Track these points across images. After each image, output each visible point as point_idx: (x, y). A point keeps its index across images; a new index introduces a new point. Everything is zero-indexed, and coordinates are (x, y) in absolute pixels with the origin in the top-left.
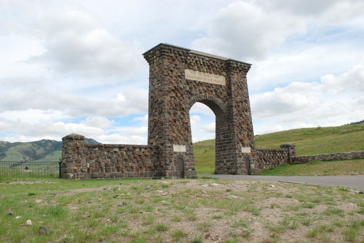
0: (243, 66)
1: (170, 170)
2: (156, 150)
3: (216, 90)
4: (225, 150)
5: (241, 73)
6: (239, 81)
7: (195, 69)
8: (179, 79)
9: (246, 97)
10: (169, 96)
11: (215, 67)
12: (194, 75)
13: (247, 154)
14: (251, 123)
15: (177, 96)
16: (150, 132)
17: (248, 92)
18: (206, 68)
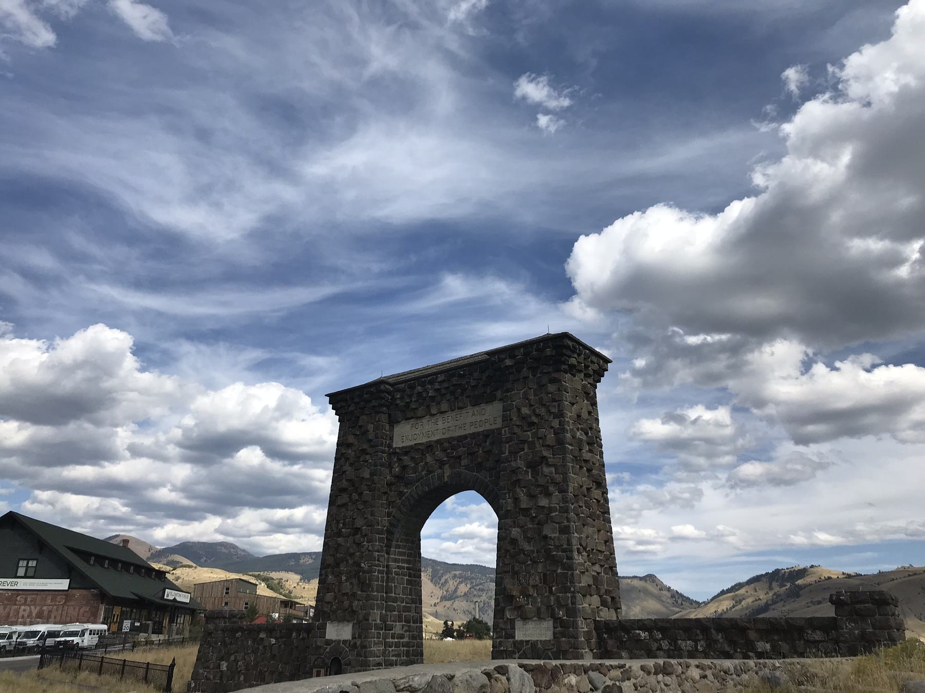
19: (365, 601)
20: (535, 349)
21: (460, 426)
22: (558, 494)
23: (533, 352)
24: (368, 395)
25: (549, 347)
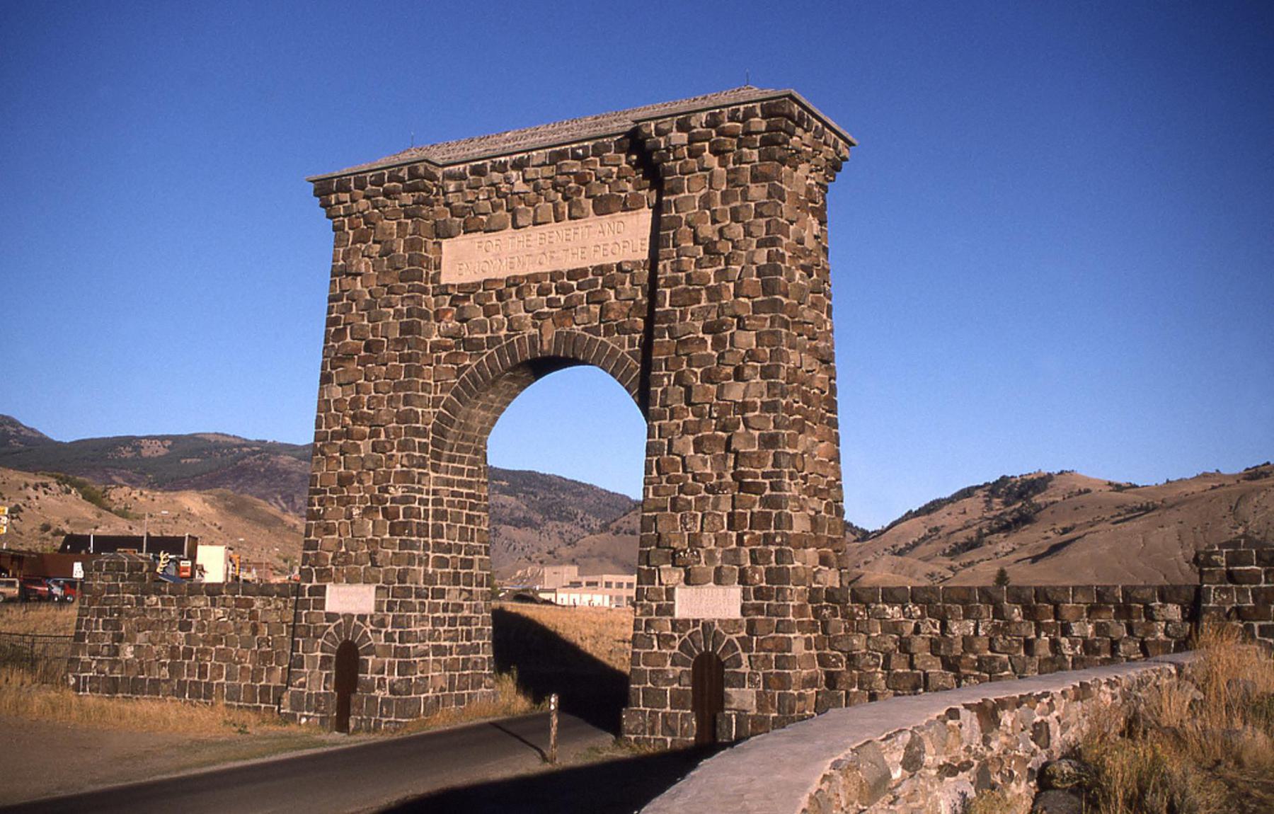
1: (303, 685)
13: (707, 626)
21: (575, 251)
22: (758, 379)
23: (722, 122)
25: (756, 116)
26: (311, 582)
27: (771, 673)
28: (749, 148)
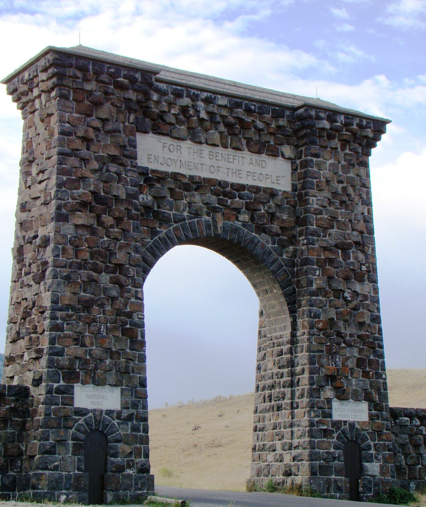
0: (355, 127)
1: (56, 468)
2: (17, 400)
3: (252, 207)
4: (279, 408)
5: (347, 151)
6: (340, 176)
7: (177, 136)
8: (113, 168)
9: (361, 232)
10: (70, 223)
11: (253, 129)
12: (173, 156)
13: (352, 425)
14: (377, 319)
15: (100, 223)
16: (10, 340)
17: (370, 212)
18: (221, 133)
19: (137, 362)
20: (357, 124)
21: (234, 171)
22: (367, 282)
24: (126, 81)
25: (370, 128)
26: (59, 382)
27: (386, 454)
28: (360, 144)
